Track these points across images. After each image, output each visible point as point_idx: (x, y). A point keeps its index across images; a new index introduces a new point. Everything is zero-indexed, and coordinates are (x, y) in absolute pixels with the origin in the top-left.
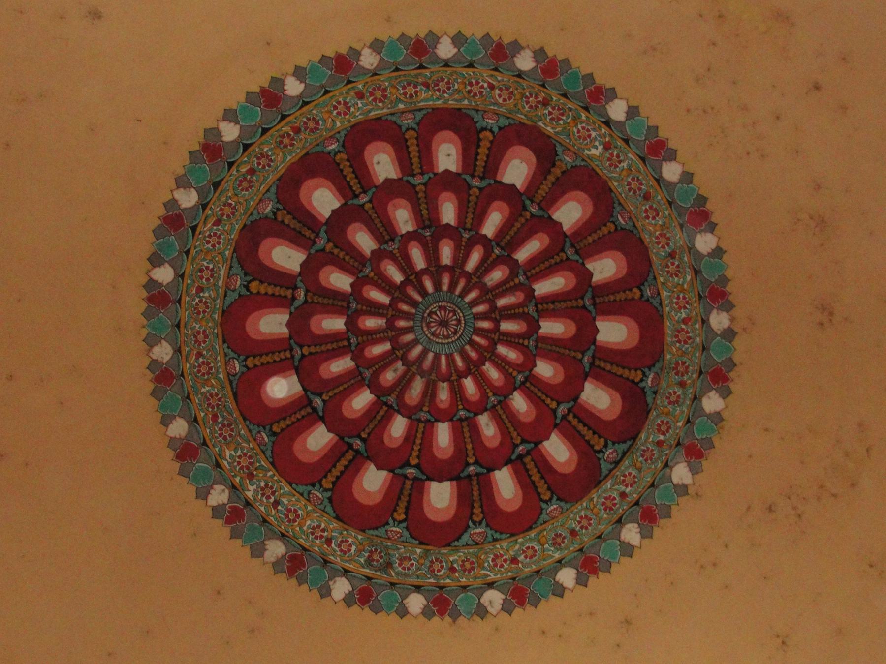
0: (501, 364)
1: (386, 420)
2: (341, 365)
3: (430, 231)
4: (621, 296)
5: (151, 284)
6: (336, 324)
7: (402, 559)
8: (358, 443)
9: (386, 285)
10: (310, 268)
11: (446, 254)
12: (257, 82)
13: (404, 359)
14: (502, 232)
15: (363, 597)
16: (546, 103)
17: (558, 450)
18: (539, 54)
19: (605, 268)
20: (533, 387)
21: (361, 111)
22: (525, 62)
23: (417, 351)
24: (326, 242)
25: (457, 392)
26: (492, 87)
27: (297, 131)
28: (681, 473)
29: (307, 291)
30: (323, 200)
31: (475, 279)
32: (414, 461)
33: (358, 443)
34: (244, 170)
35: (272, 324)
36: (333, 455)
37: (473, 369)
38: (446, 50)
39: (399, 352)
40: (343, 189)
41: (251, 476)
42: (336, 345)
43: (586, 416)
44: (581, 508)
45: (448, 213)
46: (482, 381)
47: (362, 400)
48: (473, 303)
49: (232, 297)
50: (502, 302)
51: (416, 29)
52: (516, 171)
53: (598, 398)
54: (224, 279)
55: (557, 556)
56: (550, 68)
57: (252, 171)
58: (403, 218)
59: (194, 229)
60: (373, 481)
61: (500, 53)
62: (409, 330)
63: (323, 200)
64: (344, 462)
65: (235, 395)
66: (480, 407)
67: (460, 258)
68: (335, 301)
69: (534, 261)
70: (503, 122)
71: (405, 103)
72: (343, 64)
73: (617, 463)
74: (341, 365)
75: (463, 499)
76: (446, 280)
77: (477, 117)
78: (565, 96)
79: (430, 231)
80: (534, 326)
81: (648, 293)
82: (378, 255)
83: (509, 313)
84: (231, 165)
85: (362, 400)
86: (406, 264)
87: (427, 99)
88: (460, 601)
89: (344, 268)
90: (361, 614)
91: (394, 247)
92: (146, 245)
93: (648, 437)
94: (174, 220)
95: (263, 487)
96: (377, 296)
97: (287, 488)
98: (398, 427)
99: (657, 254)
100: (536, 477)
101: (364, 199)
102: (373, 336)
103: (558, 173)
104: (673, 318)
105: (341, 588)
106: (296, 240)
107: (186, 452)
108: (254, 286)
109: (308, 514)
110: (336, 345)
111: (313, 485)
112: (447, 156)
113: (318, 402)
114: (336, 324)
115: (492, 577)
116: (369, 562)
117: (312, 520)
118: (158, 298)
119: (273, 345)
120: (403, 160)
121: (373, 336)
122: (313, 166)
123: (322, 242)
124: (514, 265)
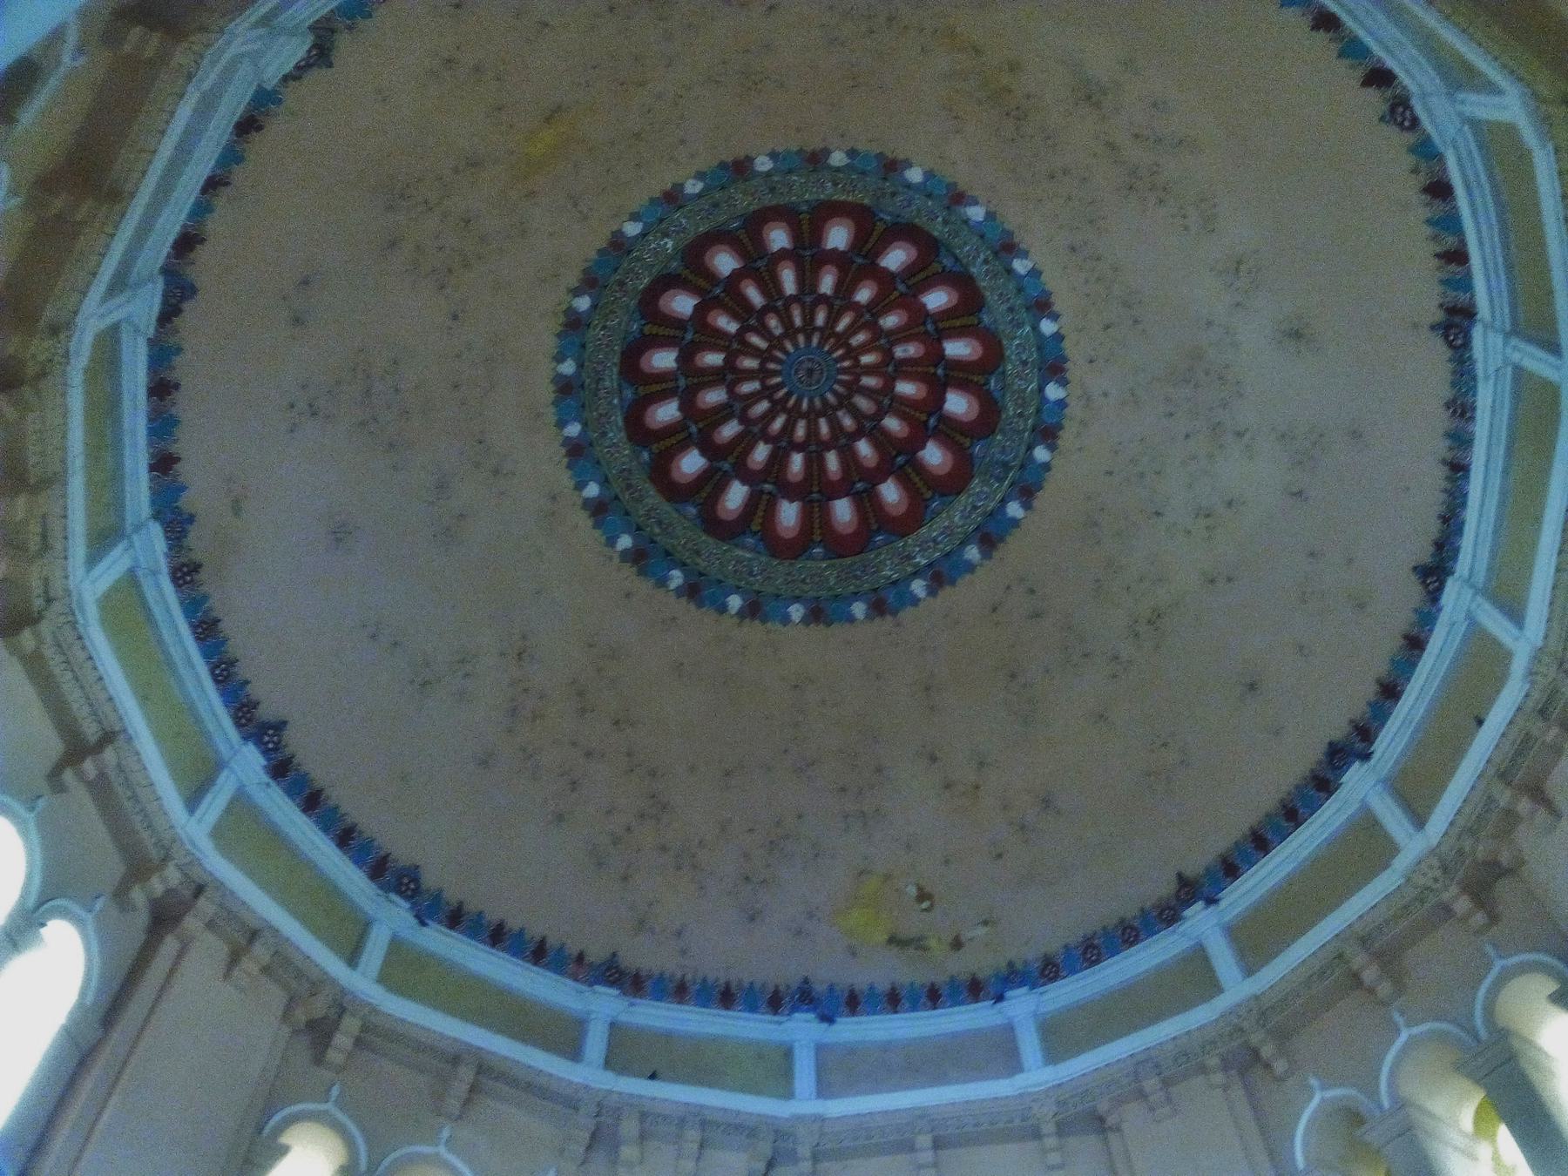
0: (853, 329)
1: (885, 433)
2: (832, 461)
3: (728, 375)
4: (805, 227)
5: (741, 614)
6: (797, 462)
7: (1003, 451)
8: (900, 460)
9: (769, 416)
10: (746, 476)
11: (749, 363)
12: (584, 520)
13: (835, 409)
14: (735, 316)
15: (1027, 494)
16: (621, 284)
17: (937, 299)
18: (576, 292)
19: (778, 238)
20: (878, 307)
21: (616, 434)
22: (583, 303)
23: (830, 397)
24: (727, 462)
25: (870, 370)
26: (604, 328)
27: (629, 486)
28: (976, 213)
29: (765, 481)
30: (691, 463)
31: (775, 342)
32: (923, 417)
33: (900, 460)
34: (657, 530)
35: (789, 514)
36: (905, 483)
37: (853, 353)
38: (568, 368)
39: (828, 411)
40: (683, 447)
41: (909, 557)
42: (815, 463)
43: (910, 271)
44: (991, 298)
45: (714, 359)
46: (865, 348)
47: (864, 448)
48: (796, 345)
49: (761, 547)
50: (798, 321)
51: (547, 393)
52: (682, 304)
53: (896, 258)
54: (745, 553)
55: (1028, 329)
56: (590, 283)
57: (660, 523)
58: (714, 397)
59: (701, 574)
60: (934, 455)
61: (574, 324)
62: (811, 401)
63: (691, 463)
64: (913, 475)
65: (840, 556)
66: (888, 355)
67: (755, 352)
68: (778, 460)
69: (764, 291)
70: (637, 316)
71: (612, 395)
72: (576, 450)
73: (957, 259)
74: (832, 461)
75: (963, 386)
76: (772, 366)
77: (631, 338)
78: (616, 270)
79: (728, 375)
80: (823, 299)
81: (805, 208)
82: (744, 419)
83: (809, 318)
84: (652, 541)
85: (864, 448)
86: (754, 397)
87: (611, 379)
88: (1050, 420)
89: (751, 448)
90: (1042, 499)
91: (738, 406)
92: (708, 616)
93: (937, 230)
94: (691, 592)
95: (922, 547)
96: (778, 424)
97: (924, 530)
98: (892, 424)
99: (769, 200)
100: (958, 323)
101: (694, 429)
102: (812, 431)
103: (690, 269)
104: (829, 192)
105: (1014, 509)
106: (721, 488)
107: (879, 608)
108: (755, 528)
109: (949, 517)
110: (815, 463)
111: (927, 507)
112: (664, 360)
113: (859, 486)
114: (797, 462)
115: (1034, 385)
116: (1000, 480)
117: (956, 515)
118: (753, 610)
119: (806, 517)
120: (663, 396)
121: (812, 431)
122: (660, 472)
123: (726, 466)
124: (766, 310)
